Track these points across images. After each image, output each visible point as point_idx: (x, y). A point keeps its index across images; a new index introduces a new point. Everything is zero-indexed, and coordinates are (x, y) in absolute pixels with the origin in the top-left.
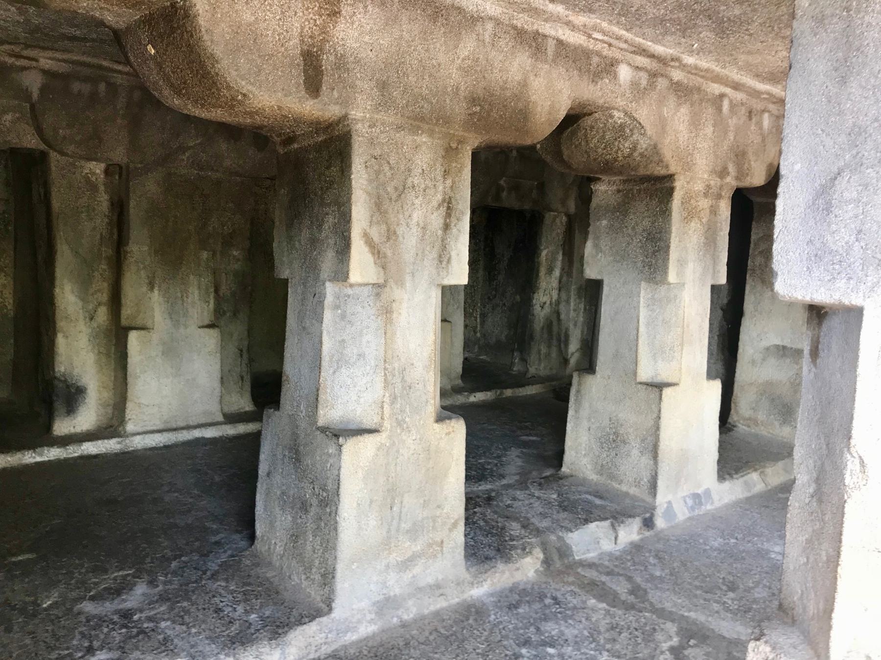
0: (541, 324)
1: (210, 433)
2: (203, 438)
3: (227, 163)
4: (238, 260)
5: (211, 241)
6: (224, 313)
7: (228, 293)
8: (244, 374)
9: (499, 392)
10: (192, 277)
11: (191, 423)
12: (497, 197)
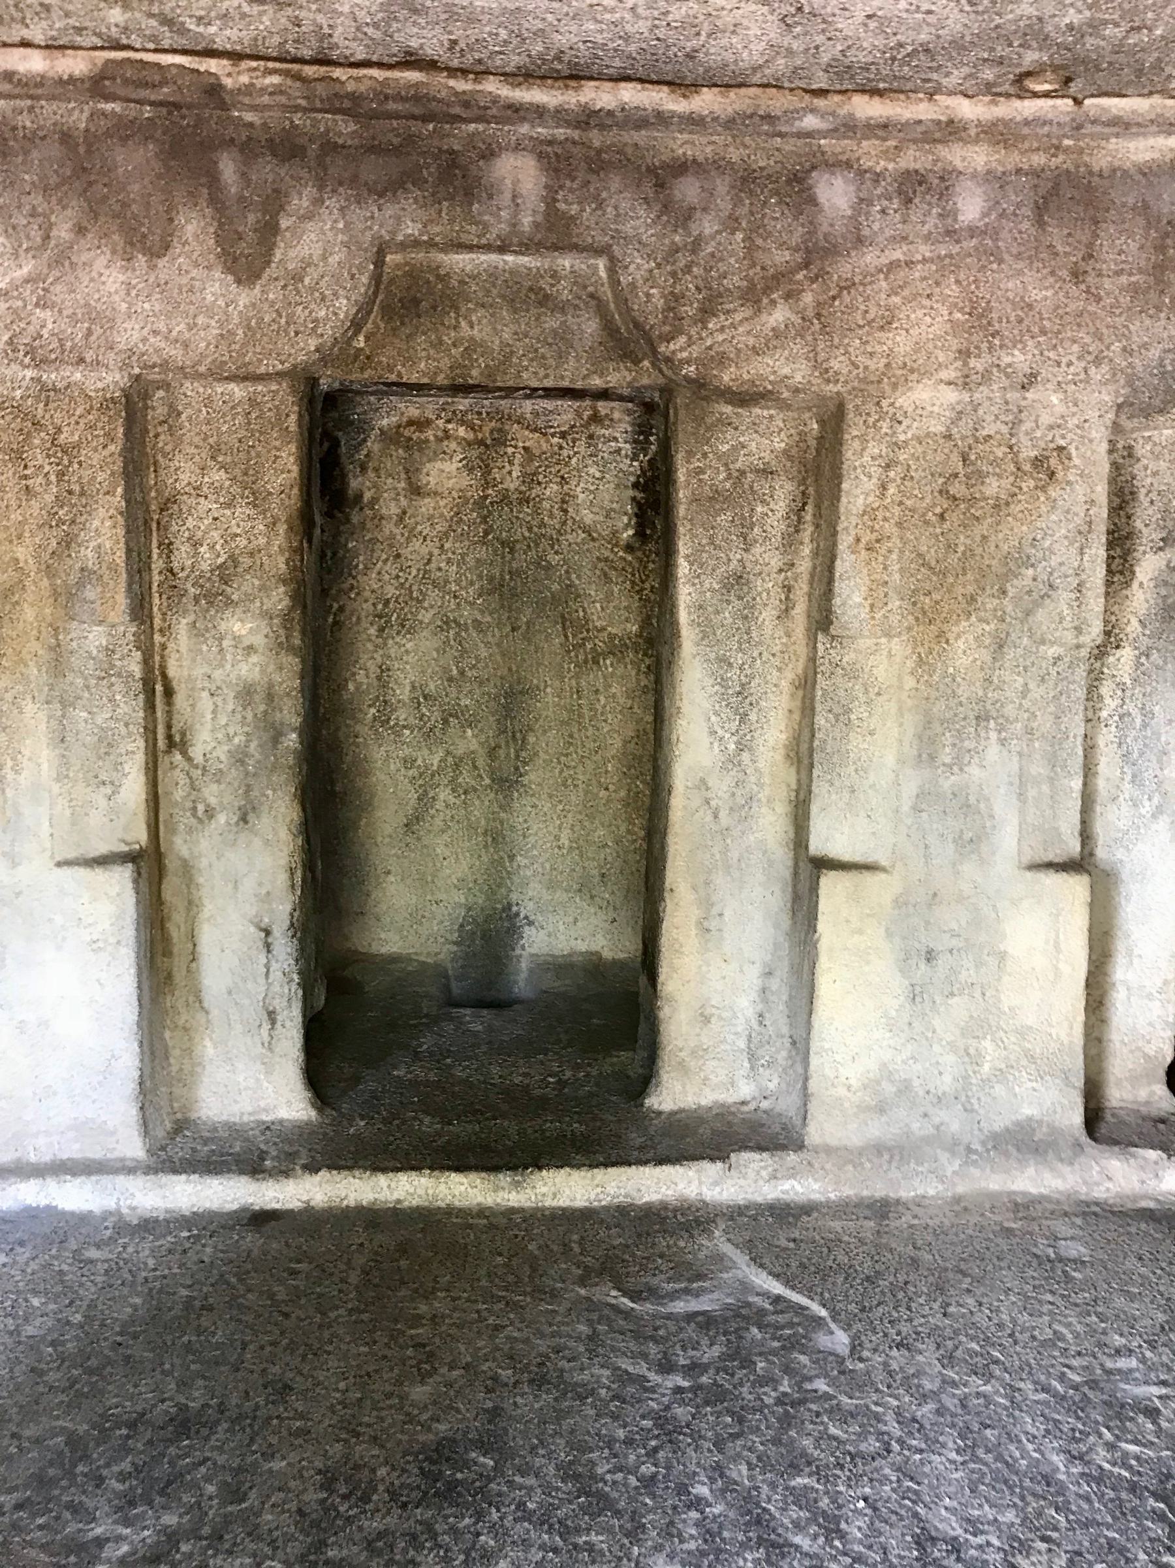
1: (75, 1197)
2: (51, 1210)
3: (130, 334)
4: (250, 649)
5: (90, 593)
6: (210, 813)
7: (222, 752)
8: (278, 1004)
10: (29, 708)
11: (33, 1158)
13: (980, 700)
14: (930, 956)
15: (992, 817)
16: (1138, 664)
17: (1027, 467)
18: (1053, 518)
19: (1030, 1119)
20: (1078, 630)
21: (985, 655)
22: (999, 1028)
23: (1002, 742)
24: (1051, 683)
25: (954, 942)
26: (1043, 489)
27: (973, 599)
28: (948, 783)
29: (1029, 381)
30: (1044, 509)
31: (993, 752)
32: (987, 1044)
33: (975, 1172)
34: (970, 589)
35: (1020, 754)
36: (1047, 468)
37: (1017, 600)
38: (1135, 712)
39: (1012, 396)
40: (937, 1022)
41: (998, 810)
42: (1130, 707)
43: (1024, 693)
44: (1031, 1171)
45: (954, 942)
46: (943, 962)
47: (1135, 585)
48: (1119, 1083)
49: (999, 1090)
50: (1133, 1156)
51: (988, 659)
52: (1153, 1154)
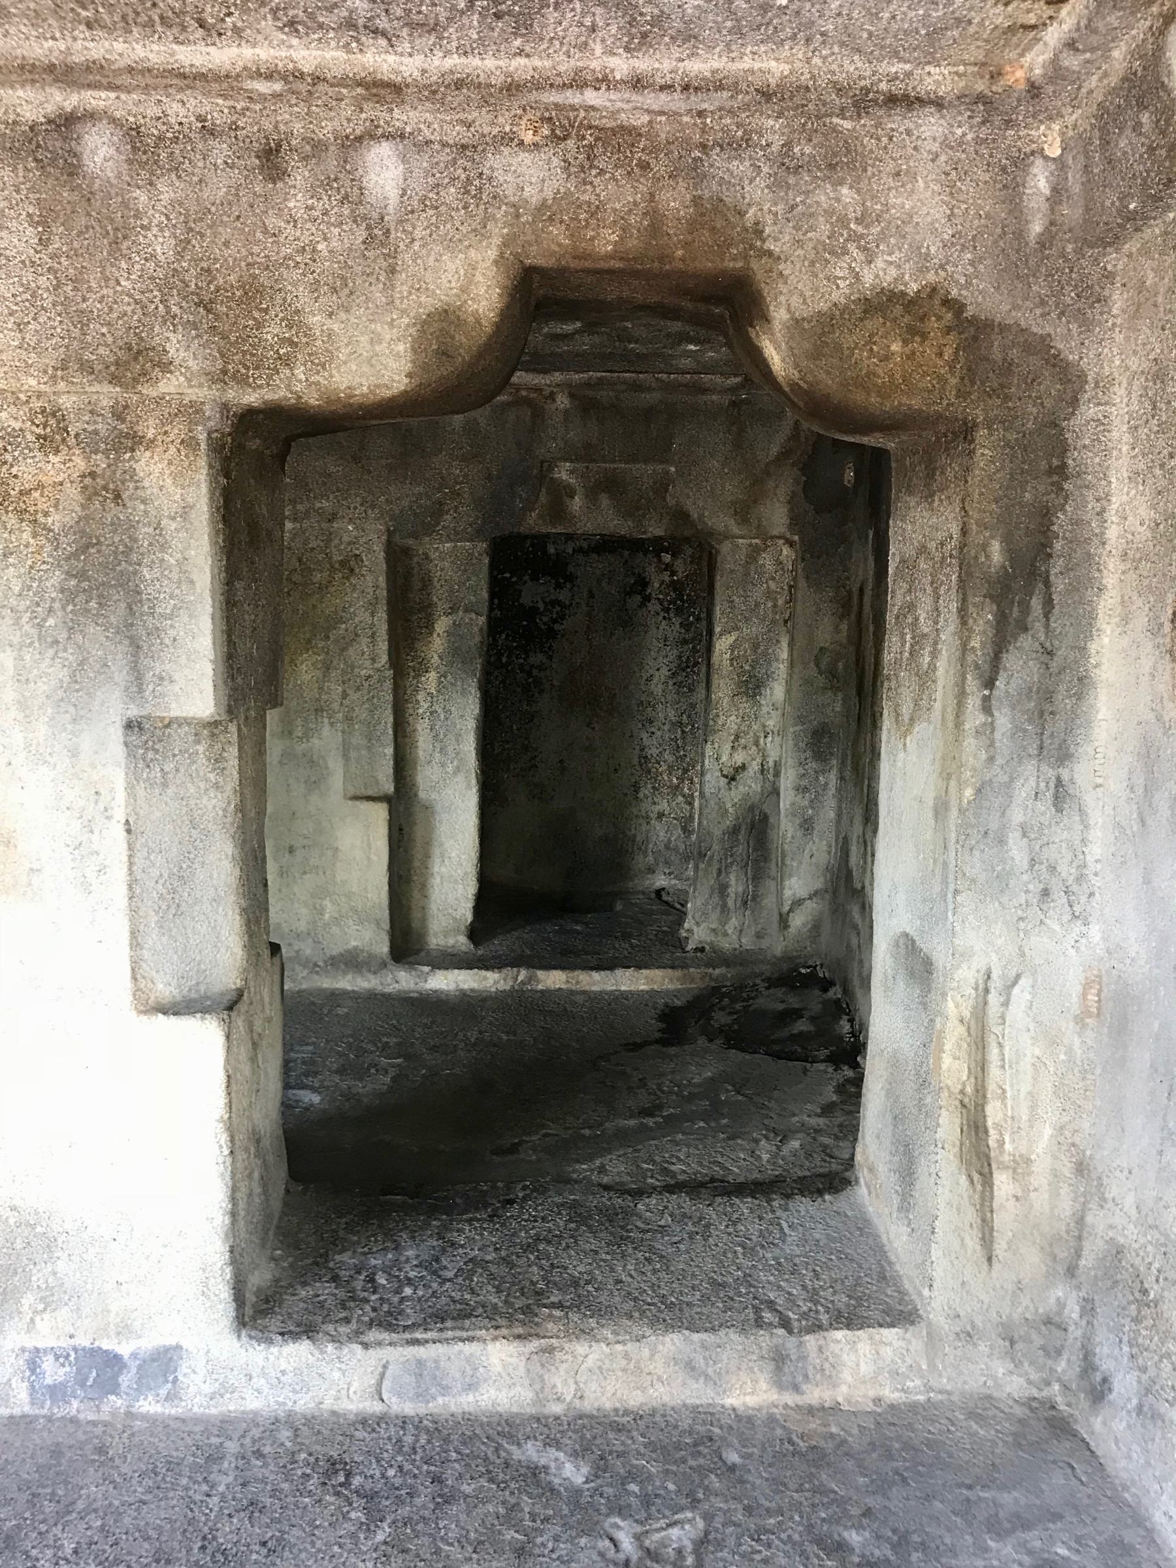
0: (729, 822)
9: (523, 974)
12: (557, 511)
13: (318, 700)
14: (291, 850)
15: (327, 768)
16: (440, 683)
17: (337, 566)
18: (355, 595)
19: (356, 948)
20: (373, 660)
21: (319, 673)
22: (335, 893)
23: (332, 724)
24: (365, 692)
25: (306, 842)
26: (348, 579)
27: (309, 641)
28: (300, 748)
29: (333, 518)
30: (348, 590)
31: (326, 730)
32: (327, 902)
33: (316, 977)
34: (308, 635)
35: (343, 732)
36: (349, 566)
37: (336, 641)
38: (439, 711)
39: (325, 525)
40: (296, 889)
41: (330, 765)
42: (436, 707)
43: (345, 695)
44: (349, 977)
45: (306, 842)
46: (299, 854)
47: (435, 635)
48: (435, 934)
49: (335, 930)
50: (416, 970)
51: (321, 676)
52: (426, 969)
